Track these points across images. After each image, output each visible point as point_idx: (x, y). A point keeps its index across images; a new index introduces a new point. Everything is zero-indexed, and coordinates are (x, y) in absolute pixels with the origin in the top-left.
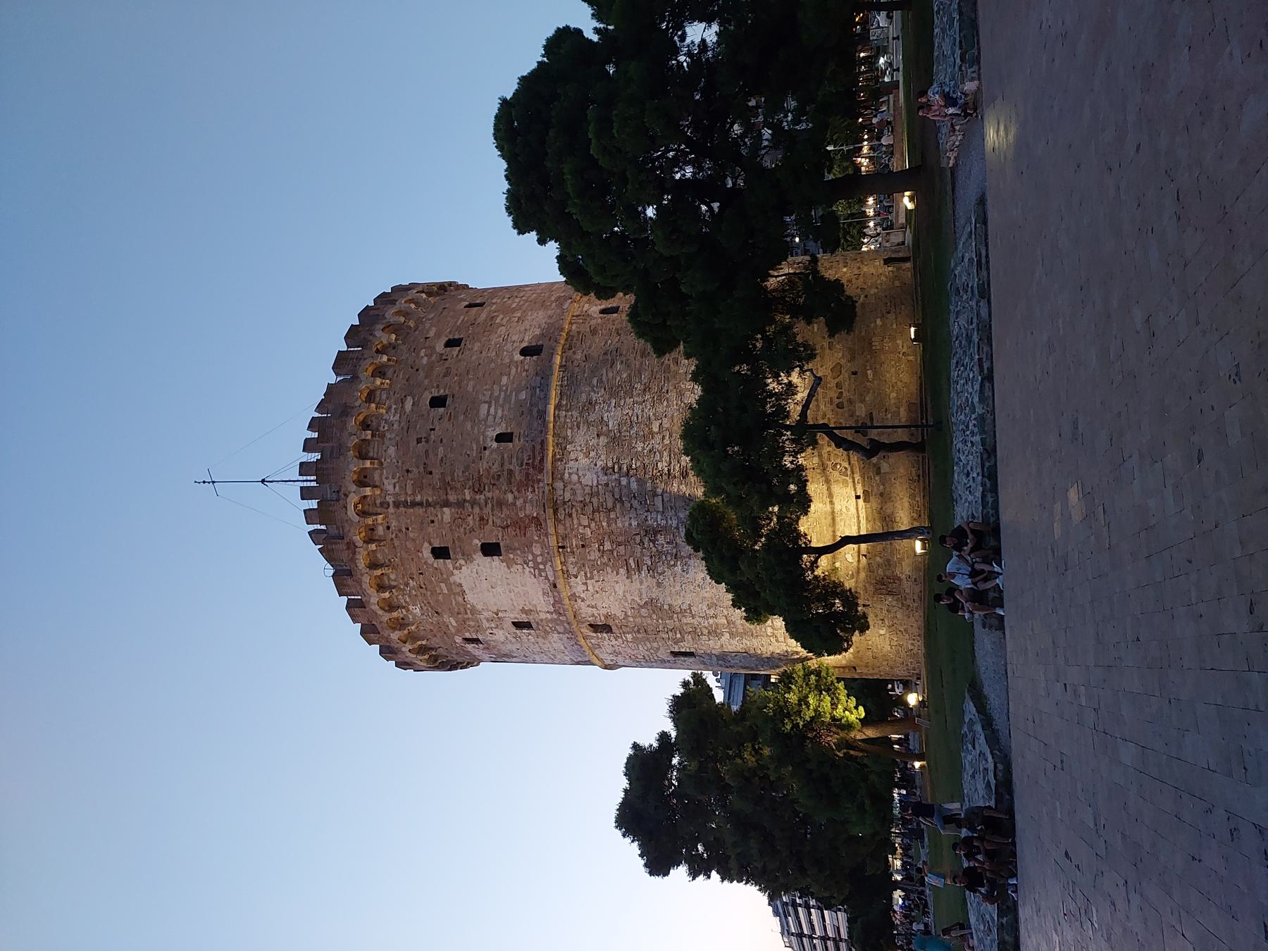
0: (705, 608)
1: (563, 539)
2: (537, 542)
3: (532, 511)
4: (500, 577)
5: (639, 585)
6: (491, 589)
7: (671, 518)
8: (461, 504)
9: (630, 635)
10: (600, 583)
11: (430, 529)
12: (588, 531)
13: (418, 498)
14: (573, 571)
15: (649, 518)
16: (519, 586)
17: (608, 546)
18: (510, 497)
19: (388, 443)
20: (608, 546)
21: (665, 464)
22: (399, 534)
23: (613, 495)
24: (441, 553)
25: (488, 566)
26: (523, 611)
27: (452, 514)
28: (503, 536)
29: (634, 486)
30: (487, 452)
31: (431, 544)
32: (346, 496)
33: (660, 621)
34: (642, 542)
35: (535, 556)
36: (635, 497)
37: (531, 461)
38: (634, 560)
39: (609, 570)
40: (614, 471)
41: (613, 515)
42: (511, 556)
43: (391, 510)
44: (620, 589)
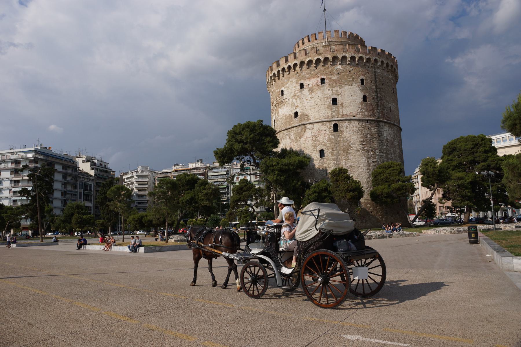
2: (369, 114)
3: (377, 114)
6: (351, 95)
11: (369, 81)
12: (372, 131)
13: (377, 79)
14: (361, 123)
16: (353, 105)
17: (369, 136)
20: (369, 136)
24: (362, 81)
26: (342, 104)
27: (374, 89)
29: (385, 147)
32: (379, 57)
33: (342, 149)
35: (364, 112)
42: (364, 105)
43: (373, 70)
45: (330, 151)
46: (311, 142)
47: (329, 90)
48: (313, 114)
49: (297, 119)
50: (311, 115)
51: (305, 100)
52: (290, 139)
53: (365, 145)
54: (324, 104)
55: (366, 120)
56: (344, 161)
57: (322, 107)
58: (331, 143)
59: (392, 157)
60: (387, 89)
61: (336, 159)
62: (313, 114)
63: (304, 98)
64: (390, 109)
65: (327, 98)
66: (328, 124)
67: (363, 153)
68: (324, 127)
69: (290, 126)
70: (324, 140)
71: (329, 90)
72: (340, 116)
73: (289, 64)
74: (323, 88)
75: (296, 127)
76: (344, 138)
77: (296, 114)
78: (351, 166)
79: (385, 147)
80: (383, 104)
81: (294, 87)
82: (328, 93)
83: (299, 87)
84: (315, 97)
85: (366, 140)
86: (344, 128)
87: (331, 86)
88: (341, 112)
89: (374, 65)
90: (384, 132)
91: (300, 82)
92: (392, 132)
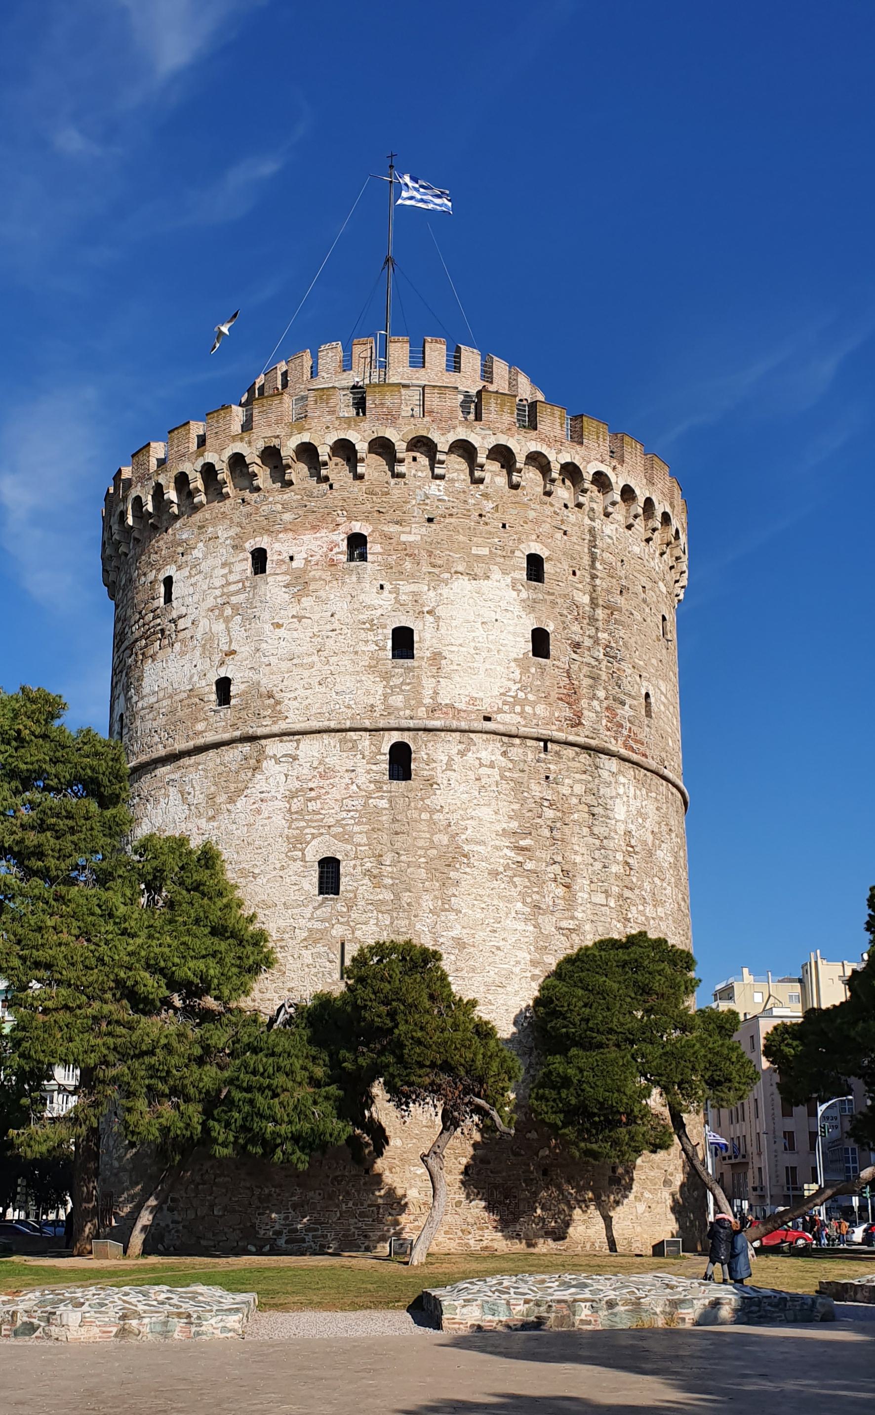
0: (454, 933)
1: (557, 753)
3: (589, 717)
4: (501, 641)
5: (493, 843)
6: (480, 620)
7: (584, 911)
8: (593, 620)
9: (387, 806)
10: (496, 789)
12: (566, 791)
13: (598, 565)
14: (516, 752)
15: (585, 882)
16: (488, 667)
17: (550, 813)
18: (601, 694)
19: (644, 543)
21: (636, 916)
22: (559, 518)
23: (605, 838)
25: (518, 629)
26: (437, 657)
28: (558, 667)
29: (614, 869)
30: (638, 678)
31: (549, 559)
34: (555, 863)
35: (533, 704)
36: (605, 867)
37: (632, 734)
38: (530, 845)
39: (516, 807)
40: (627, 845)
41: (586, 831)
42: (533, 670)
43: (587, 521)
44: (485, 813)
45: (369, 865)
46: (279, 821)
47: (382, 587)
48: (301, 692)
49: (224, 711)
50: (292, 695)
51: (268, 627)
52: (184, 800)
53: (523, 849)
54: (356, 653)
55: (538, 739)
56: (430, 919)
57: (345, 661)
58: (373, 830)
59: (647, 918)
60: (637, 616)
61: (396, 907)
62: (301, 692)
63: (266, 616)
64: (648, 705)
65: (372, 625)
66: (367, 743)
67: (516, 887)
68: (345, 754)
69: (191, 744)
70: (344, 814)
71: (382, 587)
72: (422, 712)
73: (210, 457)
74: (354, 578)
75: (217, 745)
76: (432, 812)
77: (223, 686)
78: (460, 944)
79: (614, 869)
80: (619, 678)
81: (224, 565)
82: (376, 602)
83: (248, 565)
84: (316, 617)
85: (538, 827)
86: (439, 767)
87: (395, 572)
88: (427, 692)
89: (592, 500)
90: (618, 801)
91: (250, 545)
92: (650, 808)
